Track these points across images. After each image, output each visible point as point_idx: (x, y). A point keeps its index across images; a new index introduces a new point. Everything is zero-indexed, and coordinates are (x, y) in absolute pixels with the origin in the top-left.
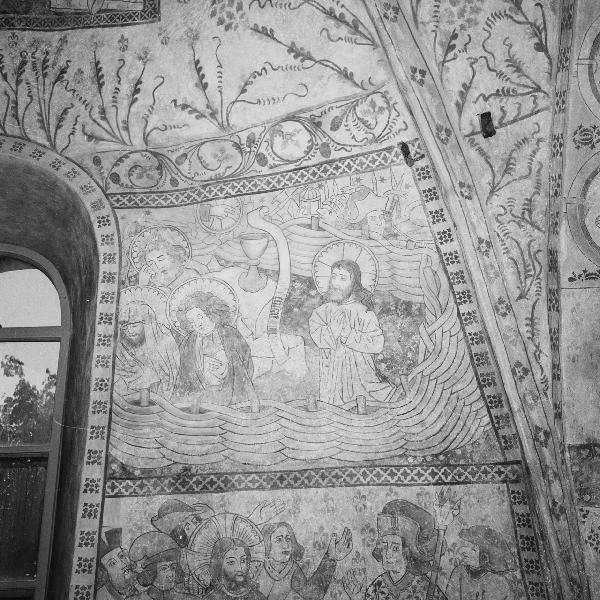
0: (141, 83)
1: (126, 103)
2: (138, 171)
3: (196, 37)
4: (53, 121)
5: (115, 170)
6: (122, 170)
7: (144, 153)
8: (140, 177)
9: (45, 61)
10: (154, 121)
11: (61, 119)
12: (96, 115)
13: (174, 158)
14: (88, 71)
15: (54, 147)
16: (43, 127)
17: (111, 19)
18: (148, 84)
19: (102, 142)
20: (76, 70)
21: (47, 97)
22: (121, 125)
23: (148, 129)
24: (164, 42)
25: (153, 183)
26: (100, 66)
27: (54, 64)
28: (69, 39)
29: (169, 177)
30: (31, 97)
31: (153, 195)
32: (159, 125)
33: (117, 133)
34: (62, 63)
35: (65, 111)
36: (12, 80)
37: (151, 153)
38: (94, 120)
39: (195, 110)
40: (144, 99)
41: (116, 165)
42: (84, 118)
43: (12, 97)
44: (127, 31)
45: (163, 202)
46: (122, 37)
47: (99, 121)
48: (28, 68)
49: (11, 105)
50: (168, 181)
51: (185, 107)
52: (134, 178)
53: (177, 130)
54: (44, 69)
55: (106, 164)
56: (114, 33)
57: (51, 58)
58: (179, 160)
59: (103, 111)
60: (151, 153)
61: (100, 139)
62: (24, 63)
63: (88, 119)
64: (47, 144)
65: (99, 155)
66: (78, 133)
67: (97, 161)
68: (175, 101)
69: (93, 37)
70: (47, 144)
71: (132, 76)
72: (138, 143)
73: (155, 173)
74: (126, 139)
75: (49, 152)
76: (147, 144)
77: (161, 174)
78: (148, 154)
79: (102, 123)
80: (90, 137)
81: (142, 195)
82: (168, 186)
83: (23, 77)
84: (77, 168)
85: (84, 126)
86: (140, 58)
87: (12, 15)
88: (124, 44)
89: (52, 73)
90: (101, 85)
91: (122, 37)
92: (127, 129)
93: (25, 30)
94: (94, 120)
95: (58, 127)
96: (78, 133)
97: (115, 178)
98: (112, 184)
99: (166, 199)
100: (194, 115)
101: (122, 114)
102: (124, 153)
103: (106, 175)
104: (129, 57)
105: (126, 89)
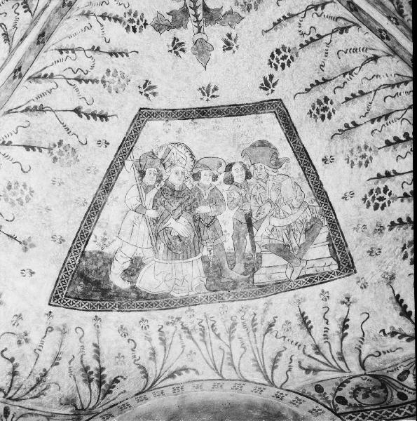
0: (348, 320)
1: (337, 338)
2: (362, 392)
3: (393, 277)
4: (268, 364)
5: (339, 394)
6: (346, 392)
7: (364, 377)
8: (365, 396)
9: (253, 320)
10: (366, 349)
11: (275, 361)
12: (310, 351)
13: (395, 376)
14: (296, 321)
15: (272, 384)
16: (259, 370)
17: (310, 281)
18: (355, 320)
19: (320, 373)
20: (283, 322)
21: (259, 345)
22: (336, 356)
23: (363, 357)
24: (364, 287)
25: (382, 400)
26: (305, 316)
27: (262, 321)
28: (273, 301)
29: (395, 393)
30: (244, 348)
31: (385, 410)
32: (372, 352)
33: (334, 364)
34: (269, 319)
35: (279, 354)
36: (225, 337)
37: (370, 375)
38: (309, 356)
39: (404, 335)
40: (353, 334)
41: (339, 389)
42: (298, 354)
43: (227, 350)
44: (326, 287)
45: (397, 415)
46: (323, 291)
47: (314, 355)
48: (239, 328)
49: (226, 356)
50: (396, 397)
51: (393, 334)
52: (360, 397)
53: (391, 354)
54: (253, 326)
55: (329, 390)
56: (317, 289)
57: (259, 318)
58: (401, 377)
59: (317, 348)
60: (370, 375)
61: (316, 371)
62: (234, 325)
63: (303, 357)
64: (266, 382)
65: (320, 383)
66: (295, 369)
67: (319, 389)
68: (383, 331)
69: (295, 296)
70: (266, 382)
71: (338, 317)
72: (355, 369)
73: (380, 392)
74: (344, 368)
75: (268, 388)
76: (365, 370)
77: (386, 391)
78: (368, 377)
79: (319, 357)
80: (308, 371)
81: (373, 412)
82: (396, 400)
83: (235, 334)
84: (300, 397)
85: (300, 362)
86: (343, 303)
87: (222, 292)
88: (325, 296)
89: (261, 328)
90: (309, 330)
91: (323, 291)
92: (342, 359)
93: (233, 301)
94: (309, 356)
95: (274, 368)
96: (295, 369)
97: (342, 400)
98: (340, 406)
99: (400, 412)
100: (404, 339)
101: (336, 348)
102: (344, 379)
103: (331, 398)
104: (332, 303)
105: (334, 327)
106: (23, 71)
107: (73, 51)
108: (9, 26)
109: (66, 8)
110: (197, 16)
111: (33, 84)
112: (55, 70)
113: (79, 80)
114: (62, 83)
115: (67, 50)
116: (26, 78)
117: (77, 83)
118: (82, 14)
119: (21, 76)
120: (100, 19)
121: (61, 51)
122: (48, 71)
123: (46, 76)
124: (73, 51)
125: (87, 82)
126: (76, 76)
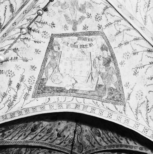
106: (142, 27)
107: (137, 7)
108: (125, 28)
109: (122, 7)
111: (147, 23)
112: (143, 15)
113: (149, 6)
114: (148, 13)
115: (137, 9)
116: (144, 26)
117: (149, 7)
119: (144, 28)
121: (137, 11)
122: (144, 17)
123: (145, 19)
124: (137, 7)
125: (149, 3)
126: (147, 7)
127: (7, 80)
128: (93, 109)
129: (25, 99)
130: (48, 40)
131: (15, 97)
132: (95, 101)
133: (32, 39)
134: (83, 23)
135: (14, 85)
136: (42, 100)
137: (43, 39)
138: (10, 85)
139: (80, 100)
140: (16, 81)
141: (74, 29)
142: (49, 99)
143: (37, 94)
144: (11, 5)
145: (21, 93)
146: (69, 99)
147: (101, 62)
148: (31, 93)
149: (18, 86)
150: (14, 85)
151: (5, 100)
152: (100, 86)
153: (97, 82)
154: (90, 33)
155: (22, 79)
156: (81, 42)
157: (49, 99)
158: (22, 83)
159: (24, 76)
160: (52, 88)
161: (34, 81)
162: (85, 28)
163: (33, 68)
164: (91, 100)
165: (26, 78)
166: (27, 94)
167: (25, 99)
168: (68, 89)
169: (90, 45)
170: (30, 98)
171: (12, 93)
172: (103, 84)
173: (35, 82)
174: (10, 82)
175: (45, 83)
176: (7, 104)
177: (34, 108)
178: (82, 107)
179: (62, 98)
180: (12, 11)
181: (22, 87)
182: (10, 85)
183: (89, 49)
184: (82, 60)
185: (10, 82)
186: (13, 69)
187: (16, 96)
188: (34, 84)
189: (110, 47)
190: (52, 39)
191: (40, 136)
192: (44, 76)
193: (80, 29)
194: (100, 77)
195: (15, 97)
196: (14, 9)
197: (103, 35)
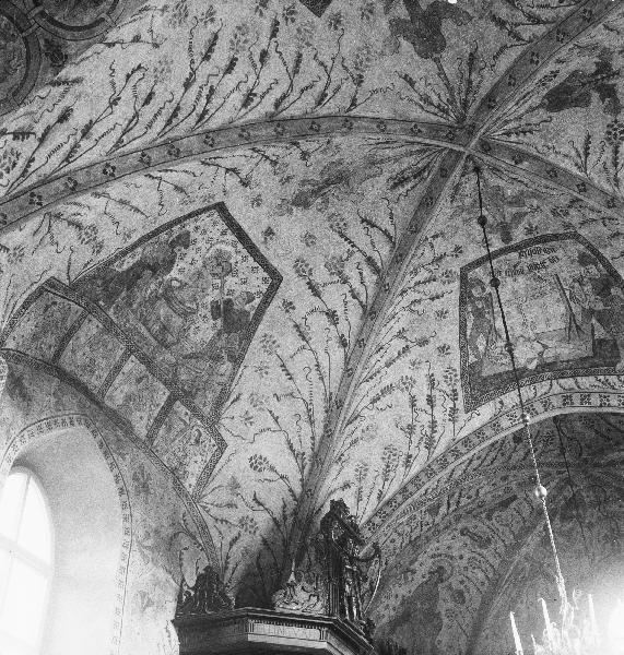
110: (603, 78)
118: (617, 186)
120: (619, 167)
127: (404, 398)
128: (604, 396)
129: (454, 421)
130: (457, 284)
131: (433, 424)
132: (602, 378)
133: (424, 297)
134: (524, 223)
135: (422, 403)
136: (486, 411)
137: (448, 287)
138: (413, 406)
139: (569, 383)
140: (421, 391)
141: (506, 237)
142: (501, 402)
143: (473, 404)
144: (370, 260)
145: (440, 414)
146: (543, 388)
147: (588, 288)
148: (460, 404)
149: (430, 401)
150: (422, 403)
151: (415, 439)
152: (601, 342)
153: (593, 335)
154: (545, 239)
155: (432, 383)
156: (526, 261)
157: (501, 402)
158: (436, 393)
159: (433, 375)
160: (497, 376)
161: (456, 376)
162: (530, 231)
163: (443, 349)
164: (592, 379)
165: (438, 377)
166: (454, 410)
167: (454, 421)
168: (532, 366)
169: (553, 260)
170: (462, 416)
171: (425, 419)
172: (608, 337)
173: (459, 377)
174: (413, 403)
175: (480, 372)
176: (423, 445)
177: (479, 432)
178: (576, 399)
179: (527, 392)
180: (377, 271)
181: (438, 402)
182: (413, 406)
183: (551, 269)
184: (543, 294)
185: (413, 403)
186: (408, 372)
187: (434, 422)
188: (459, 384)
189: (601, 258)
190: (463, 278)
191: (479, 458)
192: (472, 359)
193: (519, 235)
194: (594, 321)
195: (433, 424)
196: (379, 264)
197: (576, 237)
